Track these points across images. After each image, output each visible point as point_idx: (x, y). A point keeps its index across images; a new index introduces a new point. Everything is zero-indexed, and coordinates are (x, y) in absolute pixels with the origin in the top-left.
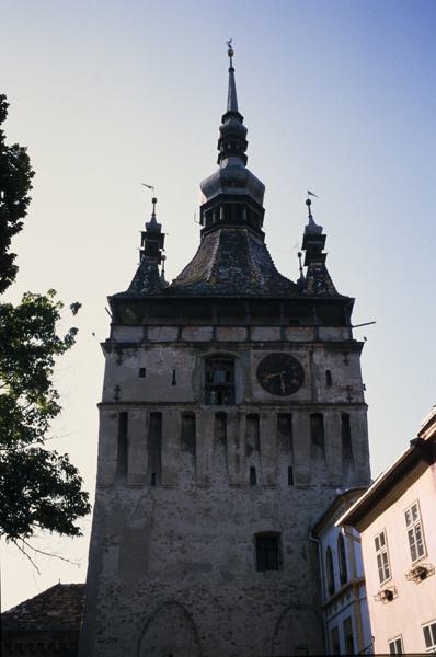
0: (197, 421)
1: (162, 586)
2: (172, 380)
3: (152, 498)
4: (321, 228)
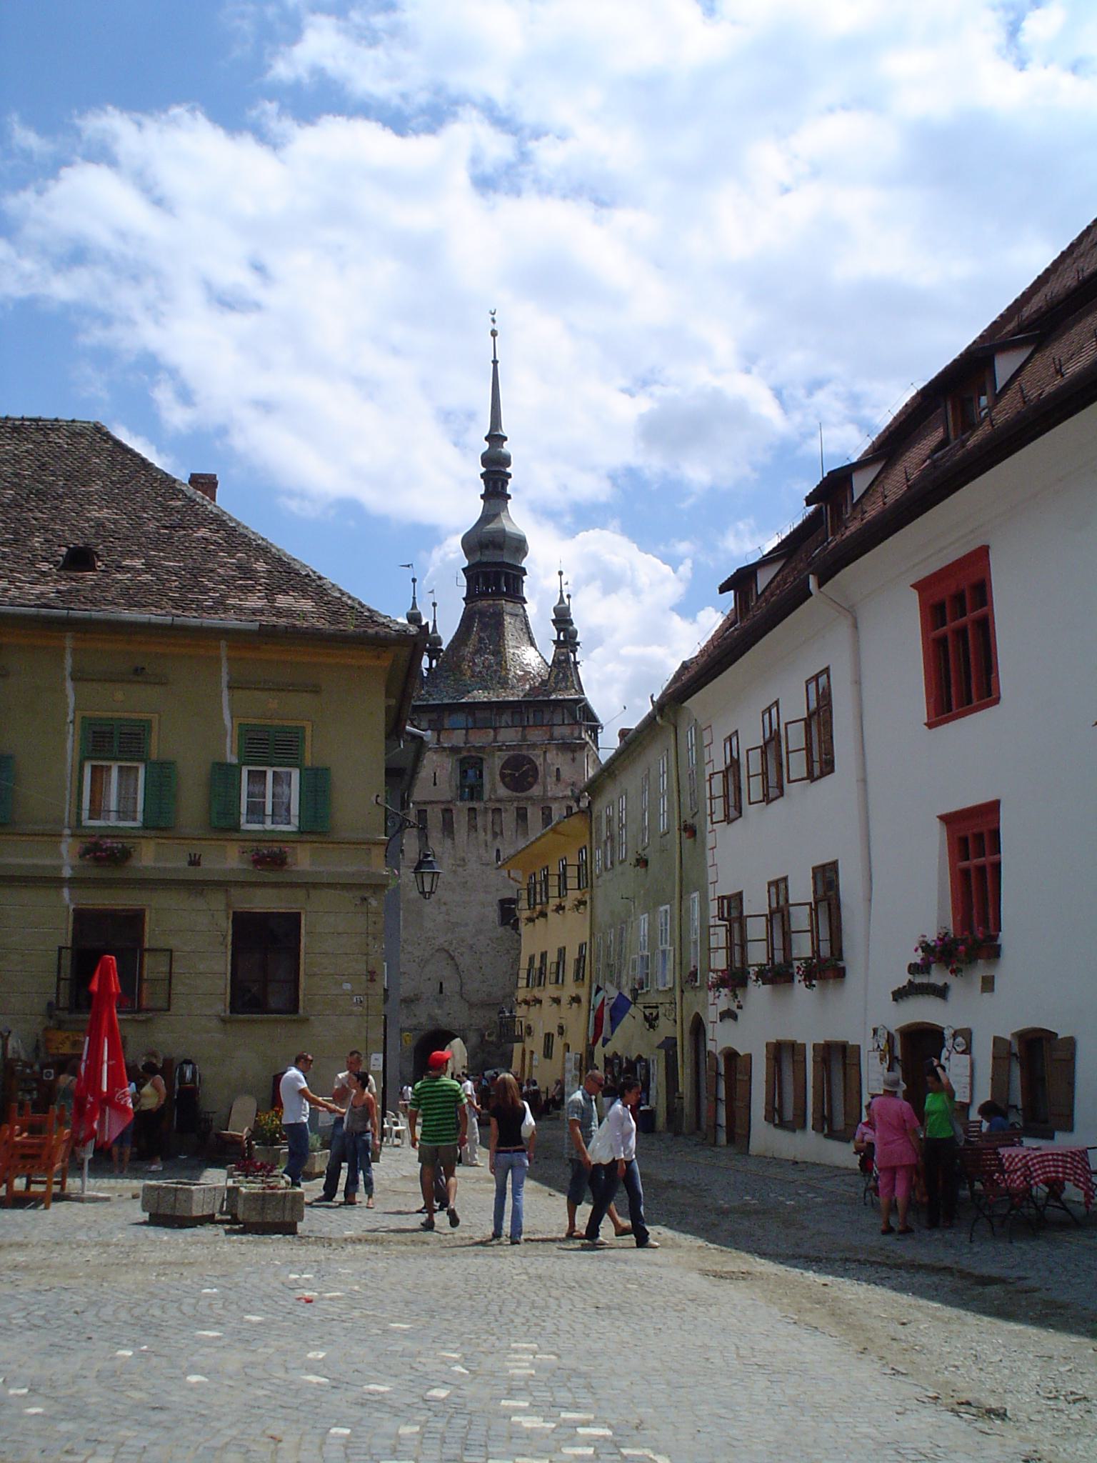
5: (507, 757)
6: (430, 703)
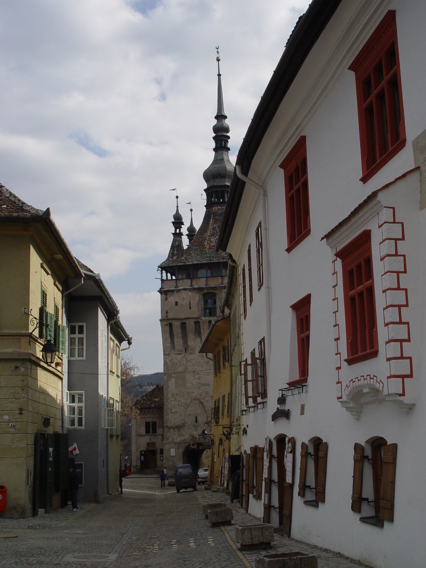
1: (192, 393)
2: (189, 307)
3: (186, 358)
6: (186, 264)
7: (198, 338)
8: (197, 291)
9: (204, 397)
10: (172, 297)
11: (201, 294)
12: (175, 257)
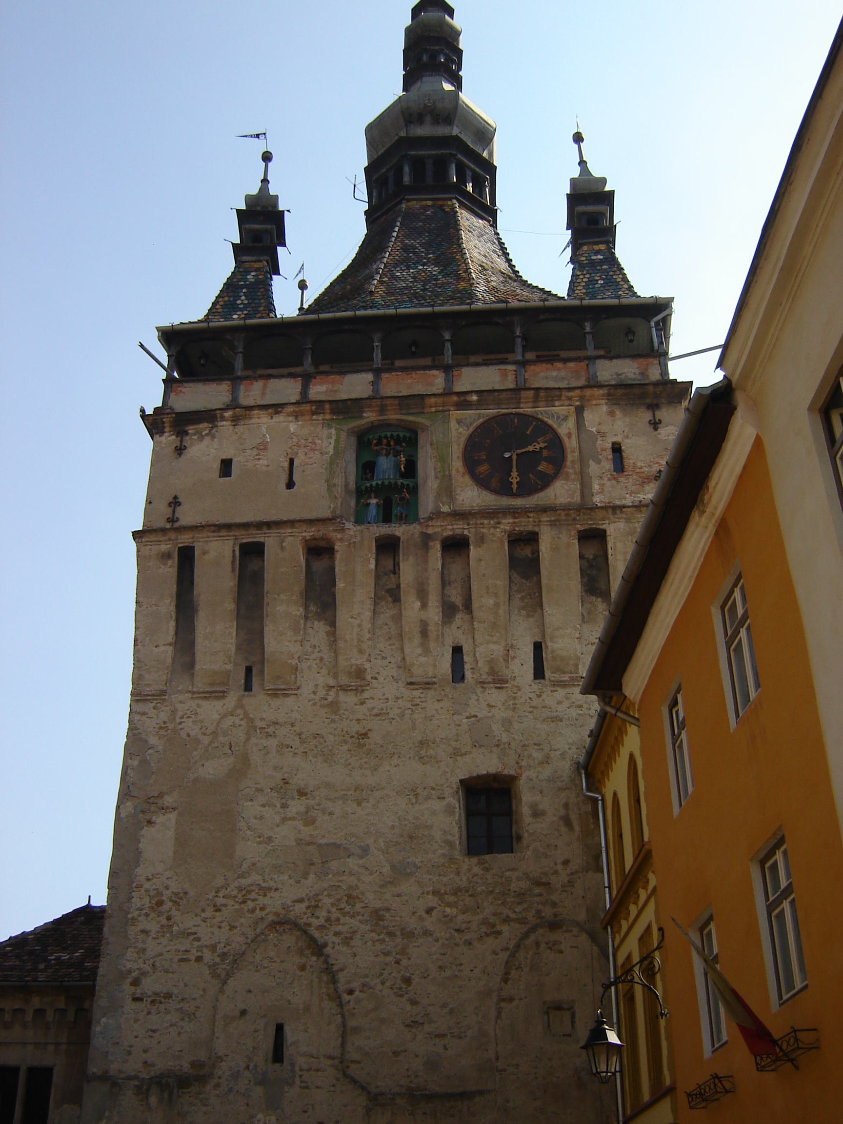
0: (338, 556)
1: (265, 891)
3: (246, 714)
4: (603, 181)
5: (481, 420)
7: (316, 623)
8: (328, 417)
9: (334, 916)
10: (207, 439)
11: (345, 428)
12: (239, 313)
